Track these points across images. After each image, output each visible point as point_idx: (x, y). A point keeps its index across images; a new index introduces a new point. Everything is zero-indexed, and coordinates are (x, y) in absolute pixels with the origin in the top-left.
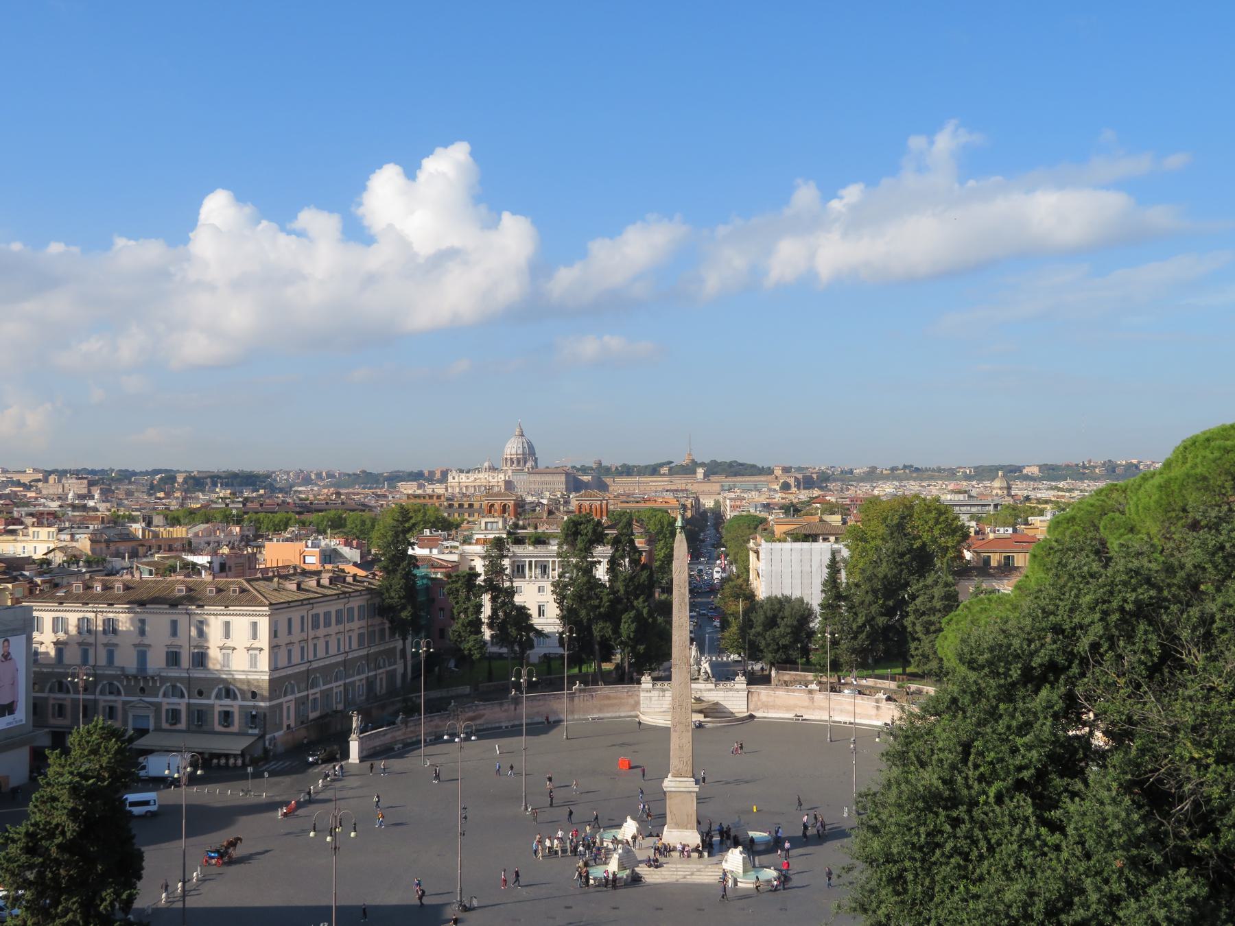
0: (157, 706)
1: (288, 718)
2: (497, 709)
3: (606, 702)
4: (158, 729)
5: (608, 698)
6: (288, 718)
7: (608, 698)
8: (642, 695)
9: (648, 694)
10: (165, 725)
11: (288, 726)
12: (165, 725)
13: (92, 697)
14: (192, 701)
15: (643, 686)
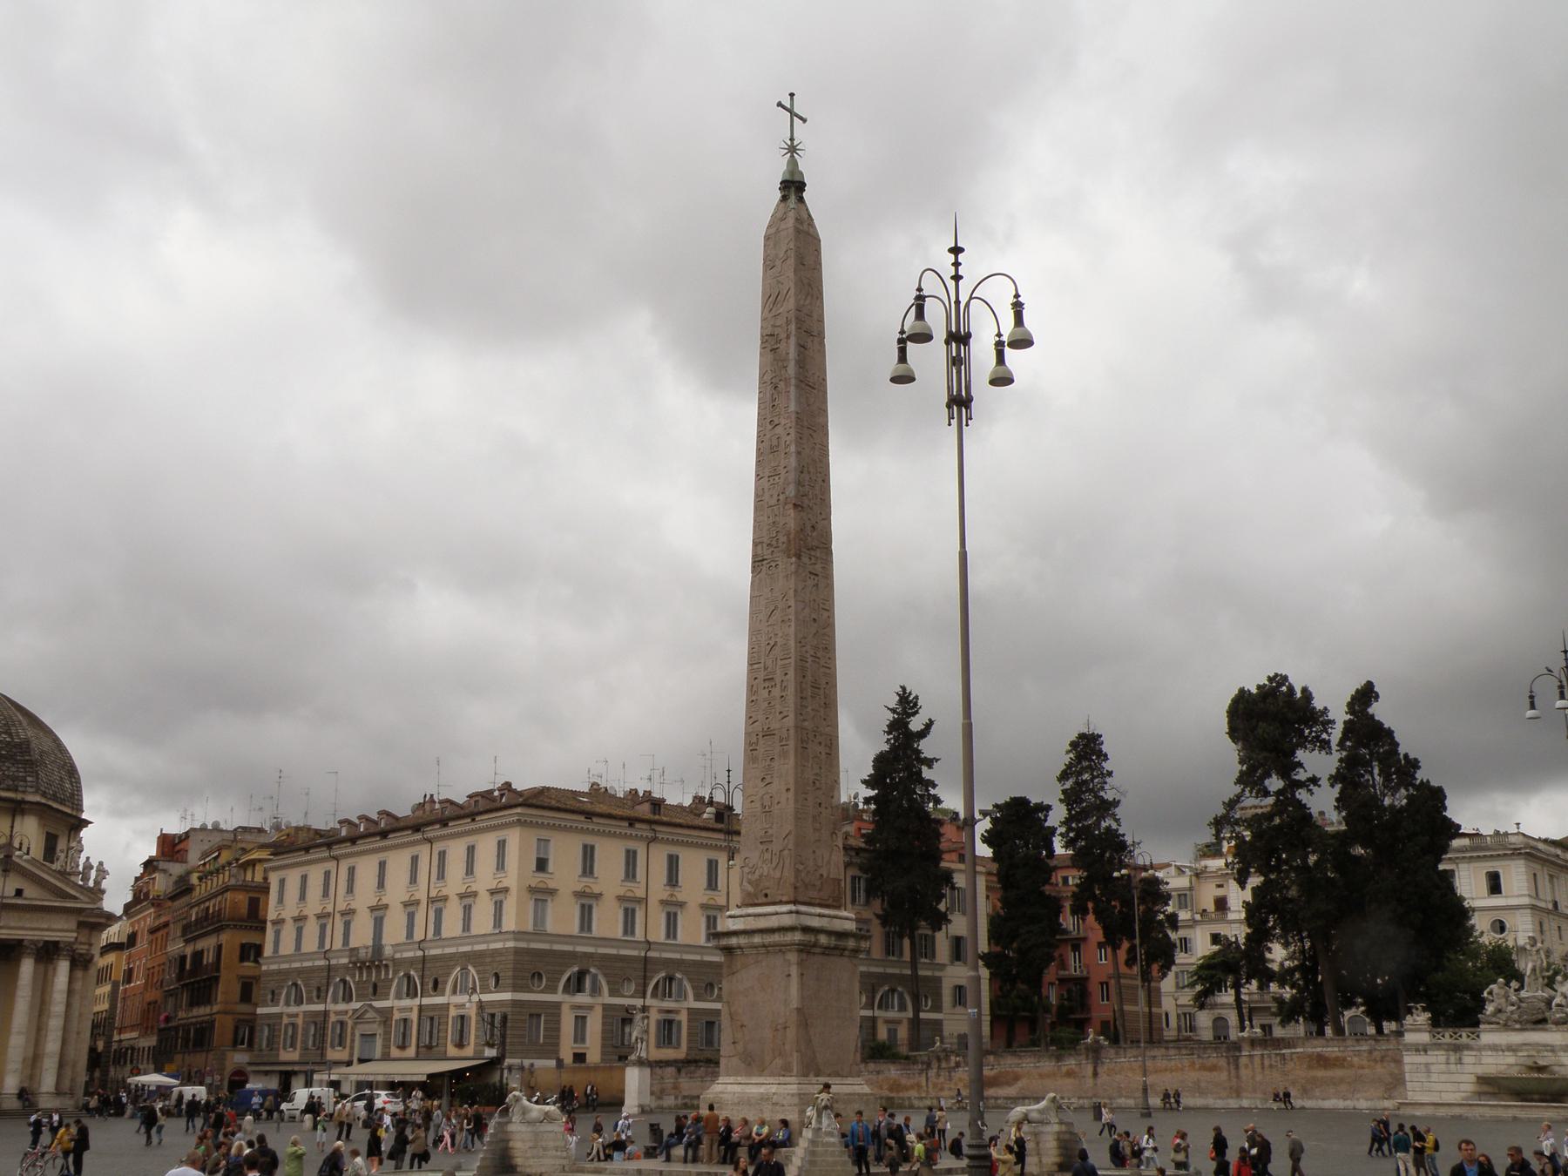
0: (386, 1014)
1: (580, 1036)
2: (1047, 1065)
3: (1320, 1073)
4: (386, 1057)
5: (1323, 1061)
6: (580, 1036)
7: (1323, 1061)
8: (1408, 1058)
9: (1421, 1059)
10: (395, 1052)
11: (580, 1057)
12: (395, 1052)
13: (321, 1007)
14: (426, 1001)
15: (1410, 1038)
